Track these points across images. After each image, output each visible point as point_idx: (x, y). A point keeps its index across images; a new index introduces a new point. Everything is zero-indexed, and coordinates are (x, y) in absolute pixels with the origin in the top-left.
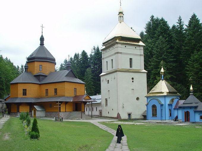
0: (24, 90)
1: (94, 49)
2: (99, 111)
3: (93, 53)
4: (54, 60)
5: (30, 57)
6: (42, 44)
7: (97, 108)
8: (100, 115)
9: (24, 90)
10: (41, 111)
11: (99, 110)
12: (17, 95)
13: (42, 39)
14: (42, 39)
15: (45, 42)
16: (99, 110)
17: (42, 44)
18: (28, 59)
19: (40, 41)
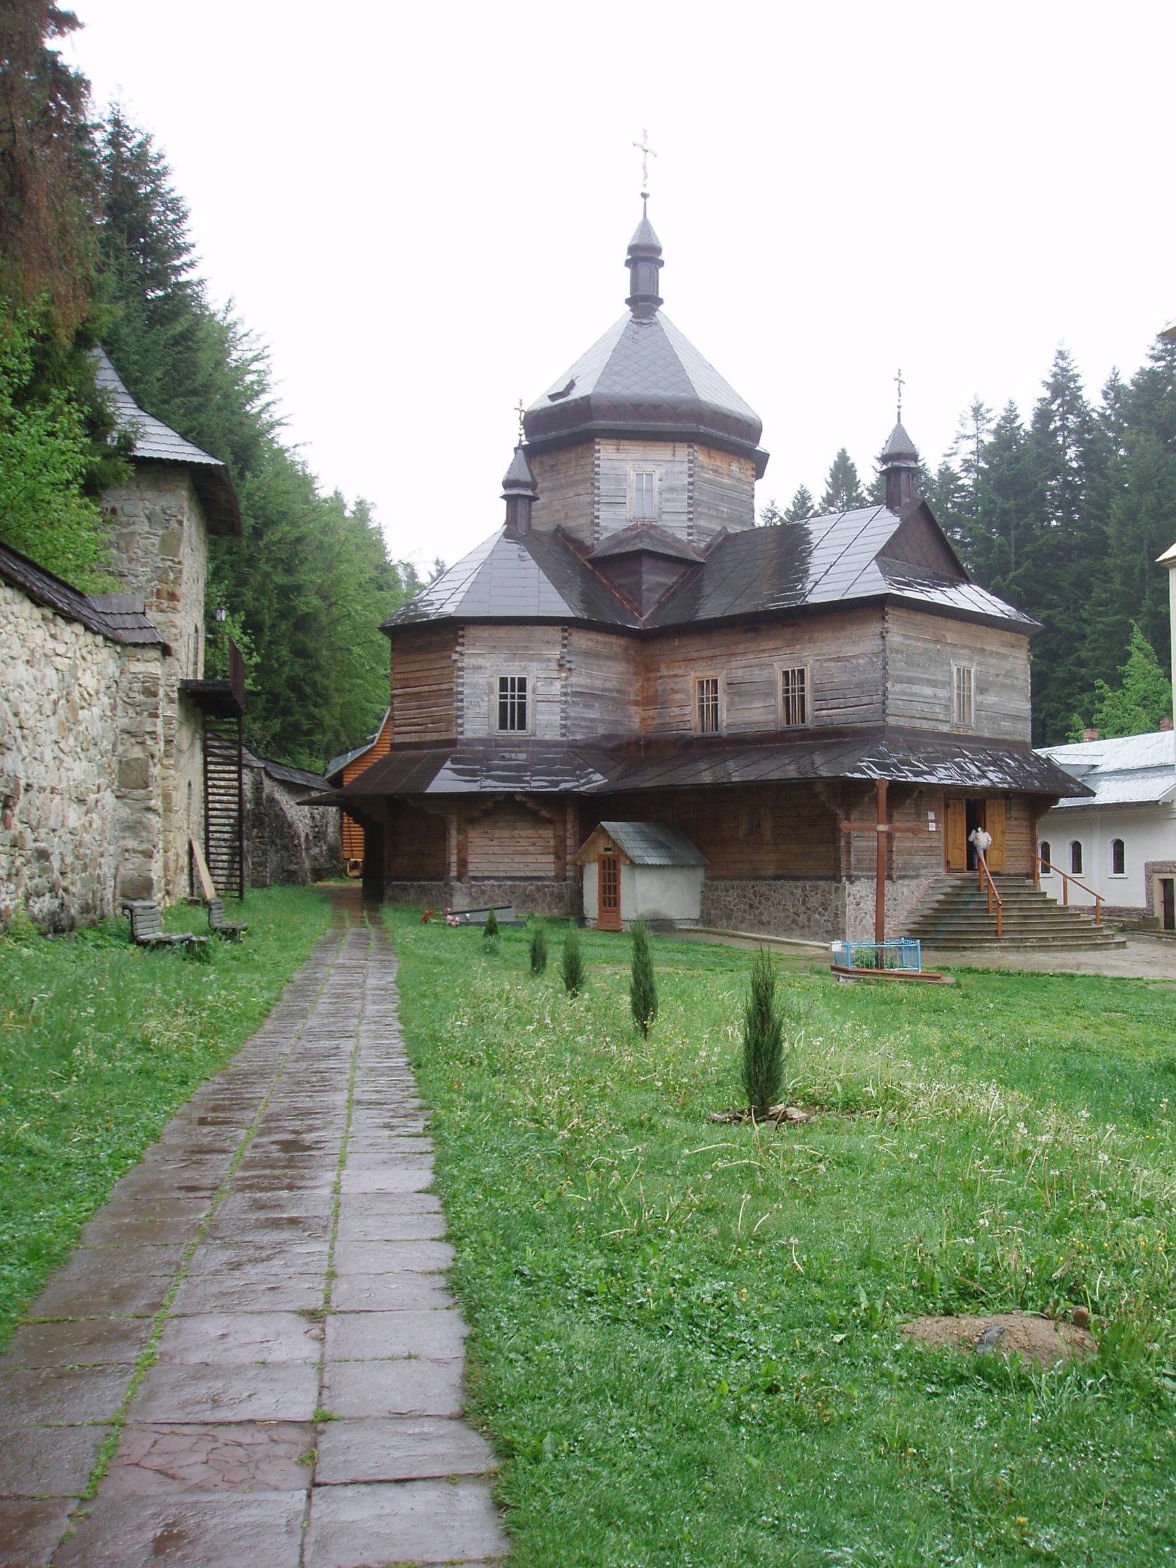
0: (501, 679)
1: (977, 412)
2: (1148, 878)
3: (971, 445)
4: (752, 430)
5: (548, 403)
6: (644, 302)
7: (1119, 846)
8: (1159, 912)
9: (501, 679)
10: (668, 874)
11: (1151, 869)
12: (452, 720)
13: (644, 257)
14: (644, 257)
15: (668, 283)
16: (1151, 869)
17: (644, 302)
18: (534, 422)
19: (628, 271)
